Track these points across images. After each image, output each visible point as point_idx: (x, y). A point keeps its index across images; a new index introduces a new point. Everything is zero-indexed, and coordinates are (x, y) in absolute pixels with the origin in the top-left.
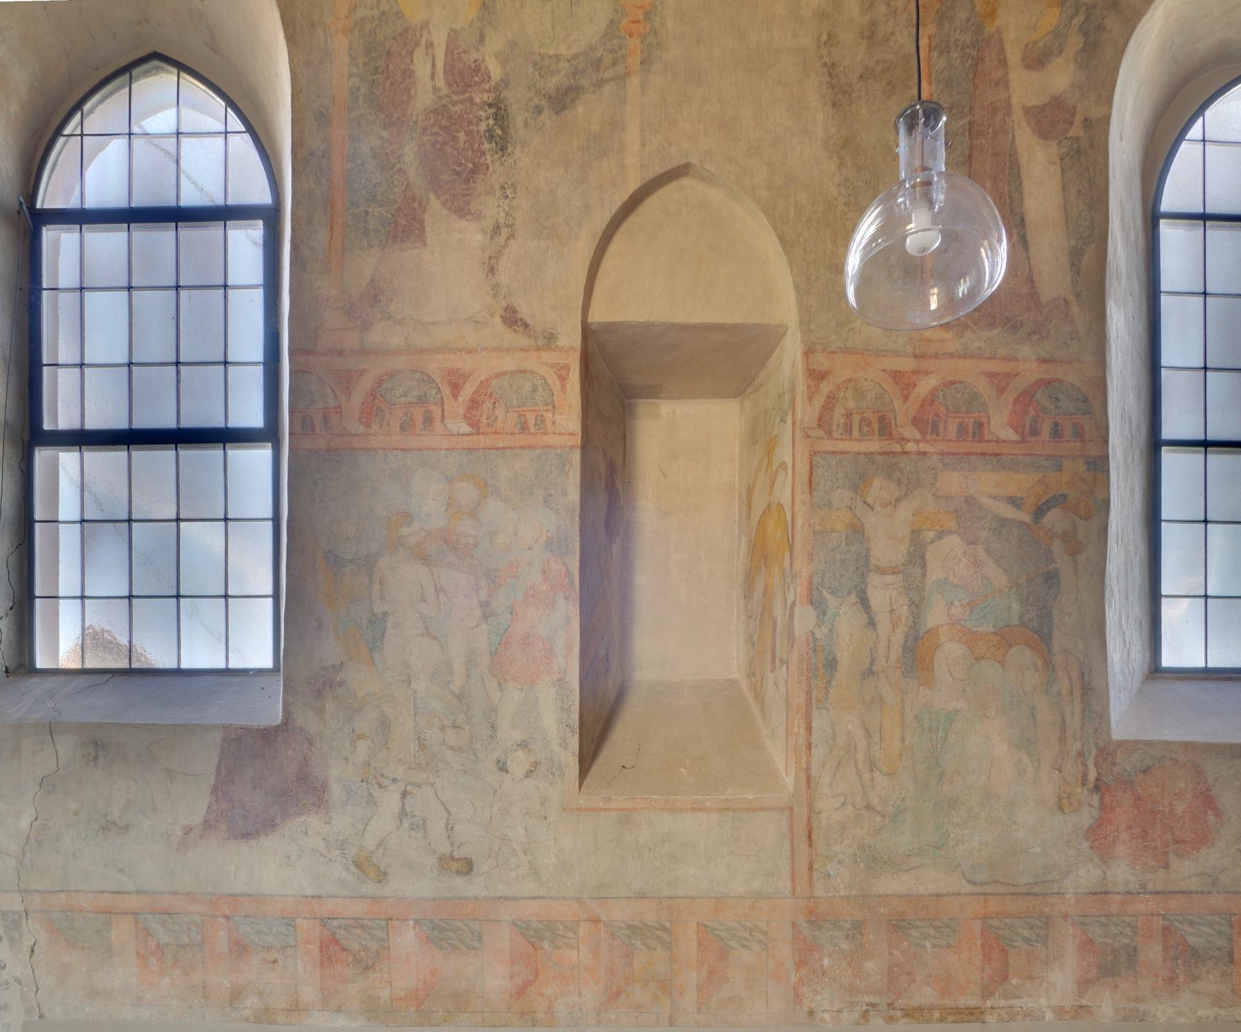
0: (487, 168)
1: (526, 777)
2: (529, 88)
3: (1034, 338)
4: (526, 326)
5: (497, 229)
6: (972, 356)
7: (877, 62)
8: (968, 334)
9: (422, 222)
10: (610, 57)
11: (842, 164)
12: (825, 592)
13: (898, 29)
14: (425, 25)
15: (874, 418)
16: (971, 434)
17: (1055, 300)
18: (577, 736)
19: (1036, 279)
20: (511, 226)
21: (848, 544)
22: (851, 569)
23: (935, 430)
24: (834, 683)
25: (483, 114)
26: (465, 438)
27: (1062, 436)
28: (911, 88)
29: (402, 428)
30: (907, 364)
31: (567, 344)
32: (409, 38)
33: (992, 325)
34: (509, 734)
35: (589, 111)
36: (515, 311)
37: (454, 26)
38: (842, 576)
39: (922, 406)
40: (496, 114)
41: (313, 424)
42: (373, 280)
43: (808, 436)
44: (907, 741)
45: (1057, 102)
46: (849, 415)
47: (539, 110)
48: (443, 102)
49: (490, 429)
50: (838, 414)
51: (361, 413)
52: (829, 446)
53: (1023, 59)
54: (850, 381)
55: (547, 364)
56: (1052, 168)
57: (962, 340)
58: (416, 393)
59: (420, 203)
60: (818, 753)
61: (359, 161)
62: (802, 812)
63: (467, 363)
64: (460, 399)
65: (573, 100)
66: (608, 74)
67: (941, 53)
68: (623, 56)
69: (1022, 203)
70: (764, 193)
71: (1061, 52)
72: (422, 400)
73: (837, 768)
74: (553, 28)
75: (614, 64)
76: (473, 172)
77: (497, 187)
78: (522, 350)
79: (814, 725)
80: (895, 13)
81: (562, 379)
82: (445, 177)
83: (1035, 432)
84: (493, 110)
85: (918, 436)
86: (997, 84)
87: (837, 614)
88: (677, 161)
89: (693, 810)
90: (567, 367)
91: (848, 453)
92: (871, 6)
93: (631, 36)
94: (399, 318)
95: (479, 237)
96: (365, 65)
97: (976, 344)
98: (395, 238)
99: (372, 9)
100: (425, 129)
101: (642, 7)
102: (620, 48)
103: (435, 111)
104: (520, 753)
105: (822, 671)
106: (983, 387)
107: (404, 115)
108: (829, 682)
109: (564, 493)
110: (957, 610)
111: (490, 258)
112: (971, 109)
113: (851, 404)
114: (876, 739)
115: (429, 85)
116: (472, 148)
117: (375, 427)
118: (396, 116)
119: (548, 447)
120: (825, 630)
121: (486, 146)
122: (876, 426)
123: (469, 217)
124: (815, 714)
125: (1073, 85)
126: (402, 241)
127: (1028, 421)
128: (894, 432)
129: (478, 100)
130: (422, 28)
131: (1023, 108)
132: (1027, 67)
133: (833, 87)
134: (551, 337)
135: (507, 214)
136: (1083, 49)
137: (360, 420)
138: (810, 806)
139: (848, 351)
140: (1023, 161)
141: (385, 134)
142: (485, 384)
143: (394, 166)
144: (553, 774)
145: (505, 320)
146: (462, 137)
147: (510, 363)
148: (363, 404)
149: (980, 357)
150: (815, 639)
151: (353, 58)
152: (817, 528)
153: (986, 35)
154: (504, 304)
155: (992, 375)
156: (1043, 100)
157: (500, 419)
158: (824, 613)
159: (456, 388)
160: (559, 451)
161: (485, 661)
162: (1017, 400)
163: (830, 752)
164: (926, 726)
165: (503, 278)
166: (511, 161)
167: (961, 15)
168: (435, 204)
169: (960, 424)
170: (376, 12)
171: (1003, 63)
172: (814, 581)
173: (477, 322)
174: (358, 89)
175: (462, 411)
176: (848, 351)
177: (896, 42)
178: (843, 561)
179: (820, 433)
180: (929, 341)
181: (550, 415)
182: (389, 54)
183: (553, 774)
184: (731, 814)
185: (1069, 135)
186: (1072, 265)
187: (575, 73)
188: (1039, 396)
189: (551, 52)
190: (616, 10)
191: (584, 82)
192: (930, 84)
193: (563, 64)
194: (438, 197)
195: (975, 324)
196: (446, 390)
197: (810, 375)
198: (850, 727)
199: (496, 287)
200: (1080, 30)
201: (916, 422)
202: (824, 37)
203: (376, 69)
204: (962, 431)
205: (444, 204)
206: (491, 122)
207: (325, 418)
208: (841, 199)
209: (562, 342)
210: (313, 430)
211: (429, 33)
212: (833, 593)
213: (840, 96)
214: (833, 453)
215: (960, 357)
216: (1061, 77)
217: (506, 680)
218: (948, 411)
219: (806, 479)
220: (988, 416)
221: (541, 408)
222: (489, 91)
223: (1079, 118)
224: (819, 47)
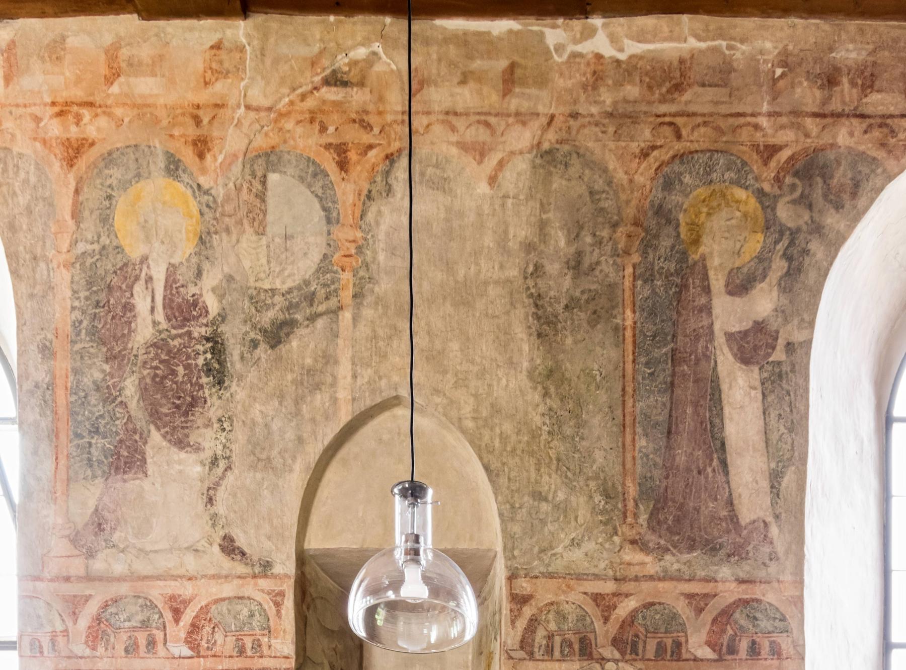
0: (205, 402)
2: (246, 322)
3: (732, 559)
4: (243, 554)
5: (214, 461)
6: (672, 579)
7: (583, 292)
8: (668, 557)
9: (143, 453)
10: (323, 291)
11: (546, 394)
13: (603, 259)
14: (144, 259)
15: (574, 639)
16: (669, 653)
17: (754, 522)
19: (735, 502)
20: (228, 458)
23: (634, 651)
25: (201, 348)
26: (186, 661)
27: (759, 654)
28: (615, 317)
29: (127, 651)
30: (609, 587)
31: (282, 572)
32: (129, 273)
33: (691, 548)
35: (302, 345)
36: (232, 540)
37: (173, 261)
39: (621, 627)
40: (213, 348)
41: (41, 647)
42: (96, 510)
43: (511, 658)
45: (759, 327)
46: (550, 637)
47: (254, 344)
48: (163, 336)
49: (210, 653)
50: (540, 636)
51: (87, 637)
53: (727, 285)
54: (552, 604)
55: (263, 591)
56: (753, 393)
57: (662, 563)
58: (140, 617)
59: (141, 434)
61: (83, 394)
63: (186, 590)
64: (181, 624)
65: (287, 335)
66: (321, 308)
67: (645, 281)
68: (336, 291)
69: (722, 428)
70: (469, 424)
71: (765, 277)
72: (145, 624)
74: (269, 262)
75: (327, 298)
76: (192, 405)
77: (214, 420)
78: (239, 577)
80: (601, 243)
82: (165, 410)
83: (732, 650)
84: (210, 345)
85: (617, 655)
86: (701, 311)
88: (388, 394)
90: (282, 594)
92: (577, 236)
93: (343, 270)
94: (122, 546)
95: (199, 468)
96: (87, 298)
97: (676, 566)
98: (117, 469)
99: (92, 243)
100: (145, 363)
101: (354, 241)
102: (333, 283)
103: (154, 345)
106: (682, 608)
107: (125, 349)
111: (209, 489)
112: (674, 336)
113: (553, 626)
115: (149, 319)
116: (191, 382)
117: (101, 650)
118: (117, 349)
121: (204, 380)
122: (576, 647)
123: (189, 449)
125: (776, 310)
126: (125, 472)
127: (725, 640)
128: (595, 652)
129: (196, 335)
130: (142, 262)
131: (725, 334)
132: (730, 293)
133: (539, 318)
134: (267, 565)
135: (224, 446)
136: (788, 274)
137: (86, 642)
139: (551, 576)
140: (724, 387)
141: (107, 367)
142: (205, 609)
143: (115, 398)
145: (223, 549)
146: (181, 370)
147: (228, 590)
148: (89, 627)
149: (679, 579)
151: (75, 292)
153: (690, 261)
154: (222, 533)
155: (690, 596)
156: (746, 325)
157: (219, 643)
159: (177, 613)
162: (714, 621)
165: (220, 508)
166: (228, 395)
167: (666, 243)
168: (156, 437)
169: (659, 644)
170: (96, 247)
171: (707, 290)
173: (196, 550)
174: (81, 322)
175: (183, 635)
176: (551, 576)
177: (601, 271)
179: (522, 654)
180: (629, 564)
181: (266, 639)
182: (110, 288)
185: (771, 359)
186: (772, 487)
187: (291, 307)
188: (737, 615)
189: (267, 286)
190: (329, 244)
191: (298, 317)
192: (634, 312)
193: (278, 299)
194: (158, 429)
195: (675, 547)
196: (168, 616)
197: (513, 599)
199: (214, 517)
200: (784, 254)
201: (616, 642)
202: (531, 269)
203: (98, 302)
204: (661, 649)
205: (164, 437)
206: (209, 356)
207: (53, 642)
208: (545, 428)
209: (277, 569)
210: (41, 652)
211: (148, 267)
213: (545, 327)
215: (660, 579)
216: (764, 302)
218: (647, 631)
220: (686, 636)
221: (258, 632)
222: (207, 326)
223: (781, 343)
224: (526, 278)
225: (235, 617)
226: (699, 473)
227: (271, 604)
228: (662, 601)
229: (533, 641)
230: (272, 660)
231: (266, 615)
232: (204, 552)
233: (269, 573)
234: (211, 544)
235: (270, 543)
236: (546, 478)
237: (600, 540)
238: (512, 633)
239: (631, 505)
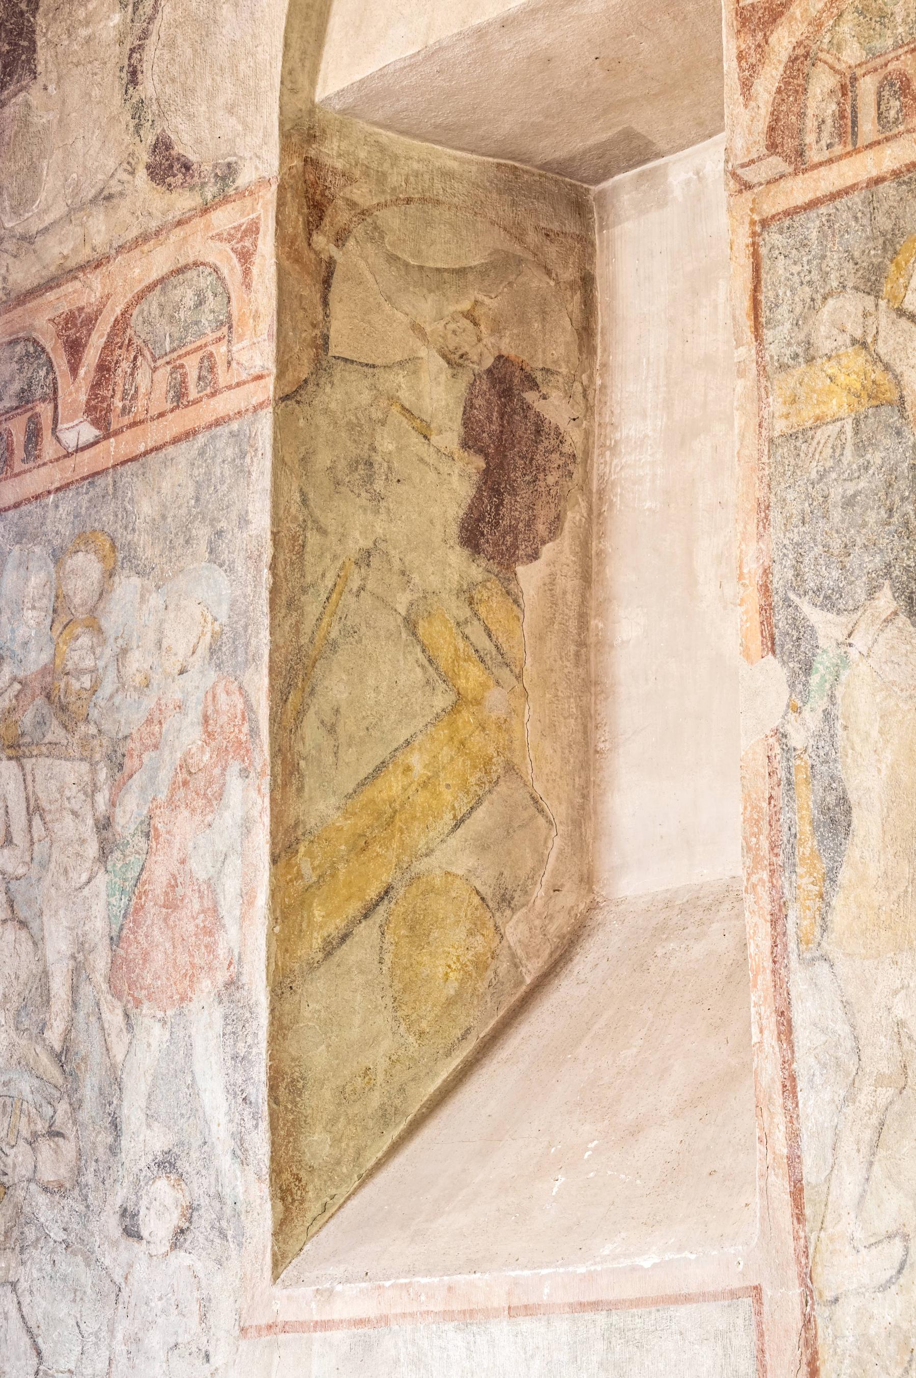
1: (174, 1246)
12: (806, 607)
18: (264, 1125)
21: (860, 448)
22: (872, 518)
24: (845, 875)
34: (144, 1140)
38: (847, 549)
46: (847, 88)
52: (799, 190)
60: (815, 1104)
62: (785, 1302)
73: (876, 1145)
79: (798, 1016)
81: (245, 257)
89: (512, 1312)
90: (253, 230)
91: (846, 191)
104: (163, 1188)
105: (808, 845)
108: (831, 876)
109: (244, 521)
119: (217, 423)
120: (812, 719)
124: (799, 981)
138: (807, 1278)
142: (122, 322)
144: (223, 1235)
150: (788, 750)
152: (780, 426)
154: (150, 139)
157: (142, 390)
158: (808, 669)
161: (100, 962)
172: (777, 583)
178: (849, 502)
179: (777, 164)
183: (223, 1235)
184: (601, 1318)
196: (61, 362)
198: (899, 1012)
212: (829, 601)
214: (813, 204)
217: (138, 1003)
219: (747, 304)
229: (802, 115)
232: (121, 194)
233: (231, 191)
234: (132, 173)
235: (233, 121)
238: (745, 116)
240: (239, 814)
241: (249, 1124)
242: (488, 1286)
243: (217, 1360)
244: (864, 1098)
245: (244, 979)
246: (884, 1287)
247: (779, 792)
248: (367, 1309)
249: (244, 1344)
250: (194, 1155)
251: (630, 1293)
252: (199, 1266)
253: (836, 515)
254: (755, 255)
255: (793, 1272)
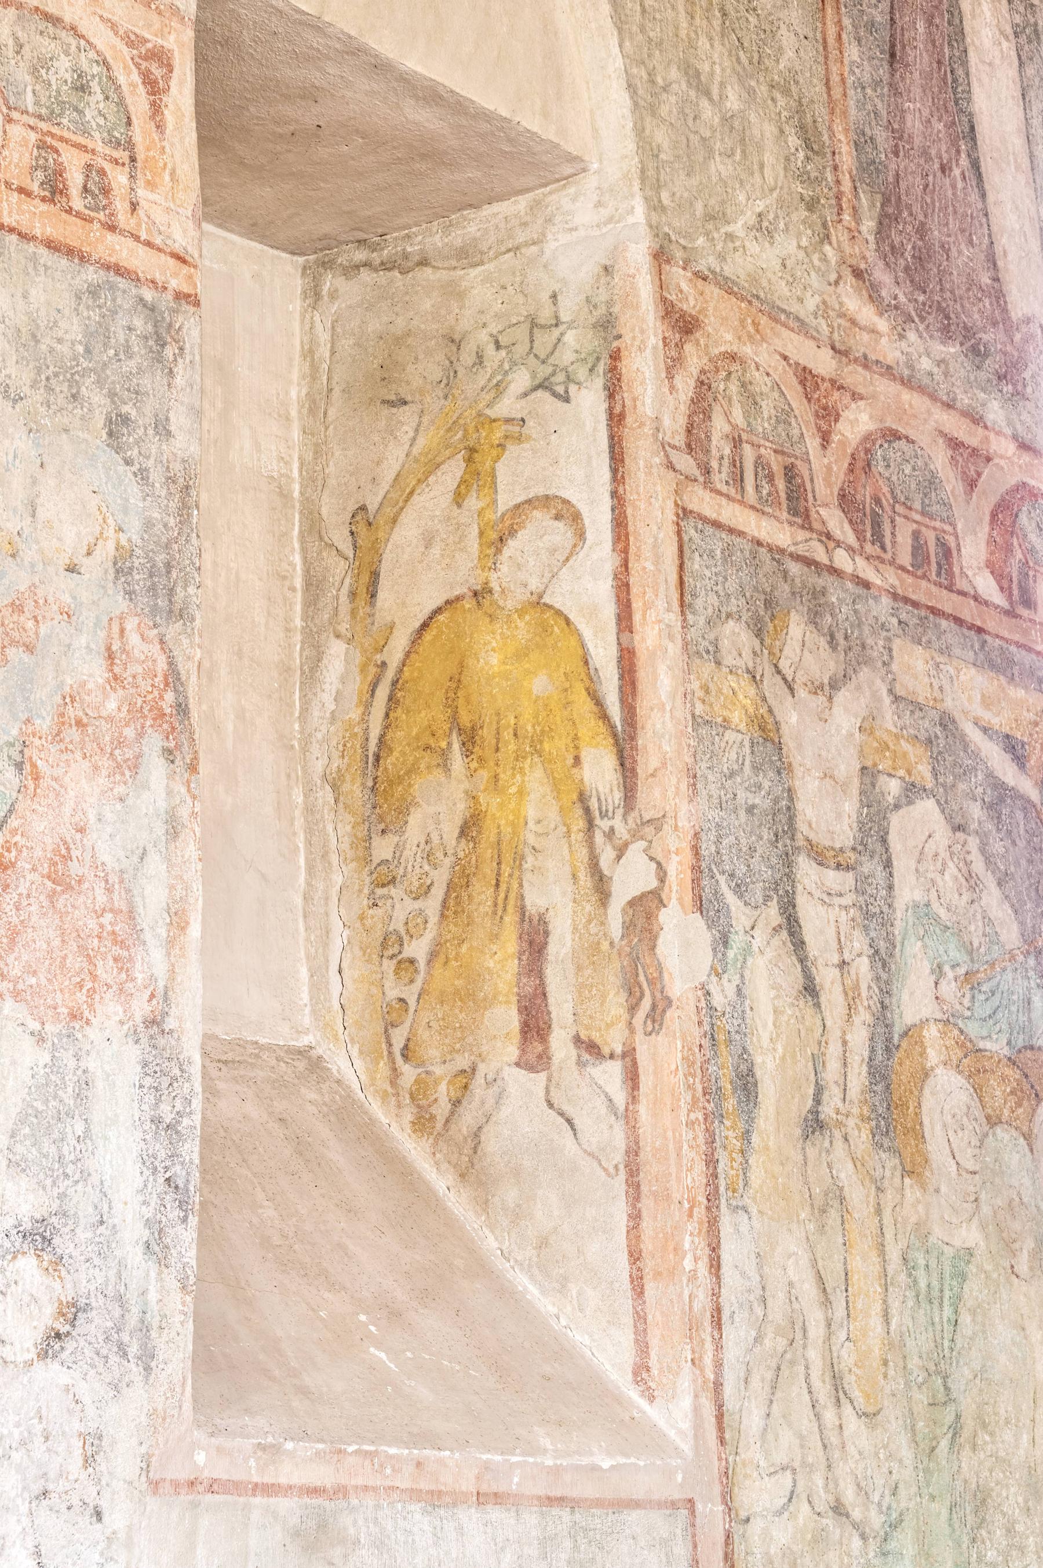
19: (1000, 264)
24: (755, 1139)
38: (752, 849)
44: (894, 1323)
55: (114, 27)
81: (154, 88)
87: (747, 951)
89: (482, 1498)
110: (949, 989)
114: (840, 1312)
119: (118, 270)
160: (148, 295)
163: (758, 1339)
164: (923, 1284)
184: (565, 1514)
225: (34, 71)
226: (943, 169)
227: (136, 78)
228: (912, 434)
230: (141, 250)
231: (121, 103)
236: (703, 42)
237: (804, 242)
239: (847, 186)
240: (162, 805)
241: (176, 1214)
242: (456, 1467)
243: (116, 1519)
244: (767, 1342)
245: (170, 1023)
246: (779, 1513)
247: (706, 1043)
248: (323, 1475)
249: (152, 1503)
250: (83, 1235)
251: (588, 1490)
252: (83, 1389)
253: (742, 814)
254: (679, 533)
255: (717, 1489)
